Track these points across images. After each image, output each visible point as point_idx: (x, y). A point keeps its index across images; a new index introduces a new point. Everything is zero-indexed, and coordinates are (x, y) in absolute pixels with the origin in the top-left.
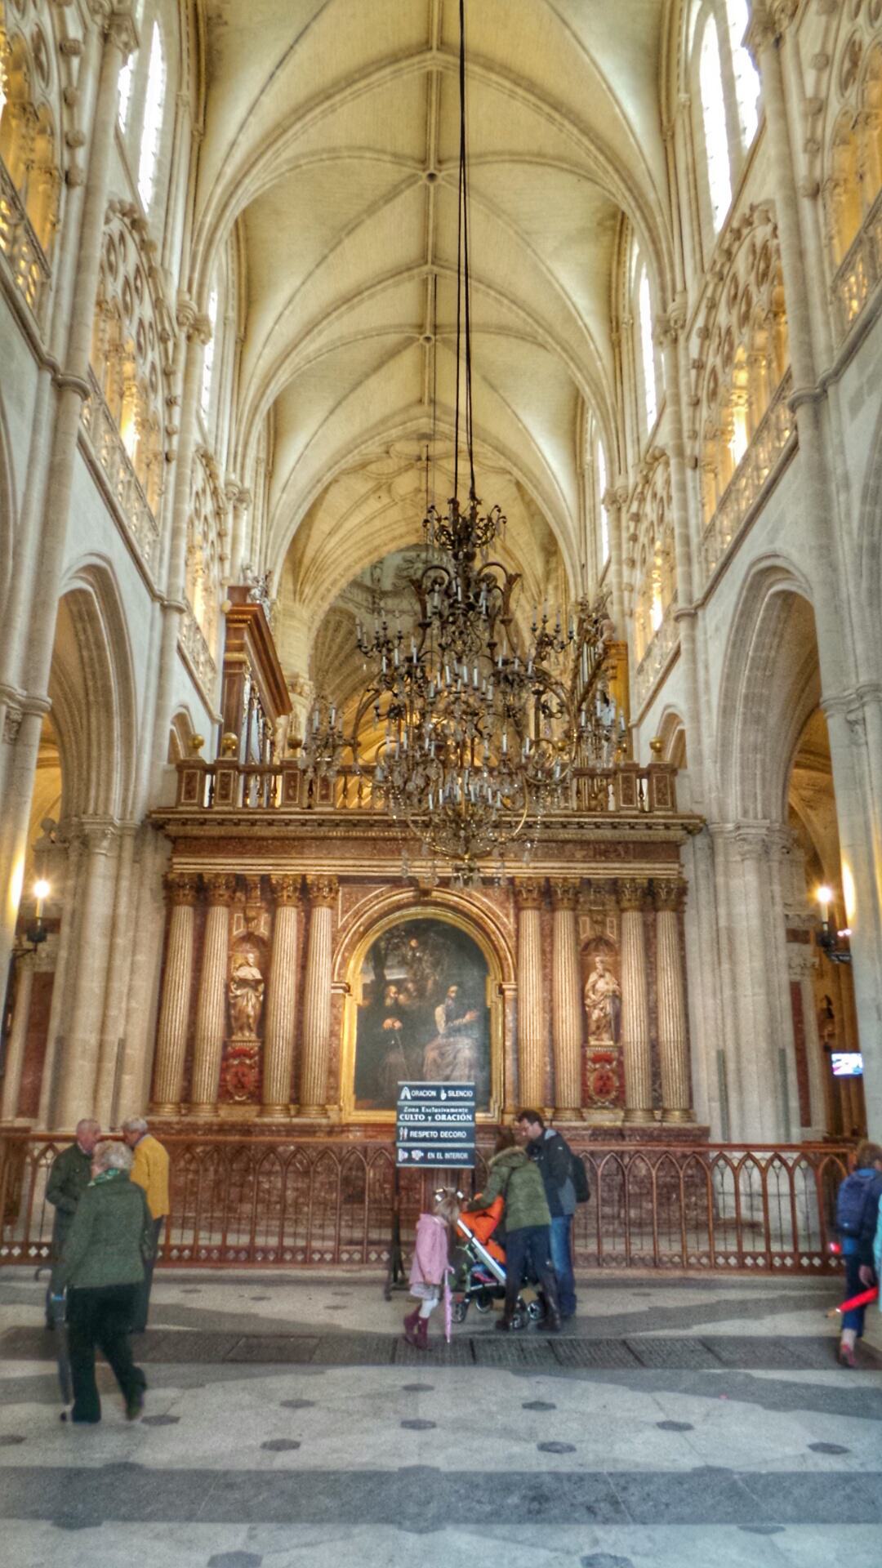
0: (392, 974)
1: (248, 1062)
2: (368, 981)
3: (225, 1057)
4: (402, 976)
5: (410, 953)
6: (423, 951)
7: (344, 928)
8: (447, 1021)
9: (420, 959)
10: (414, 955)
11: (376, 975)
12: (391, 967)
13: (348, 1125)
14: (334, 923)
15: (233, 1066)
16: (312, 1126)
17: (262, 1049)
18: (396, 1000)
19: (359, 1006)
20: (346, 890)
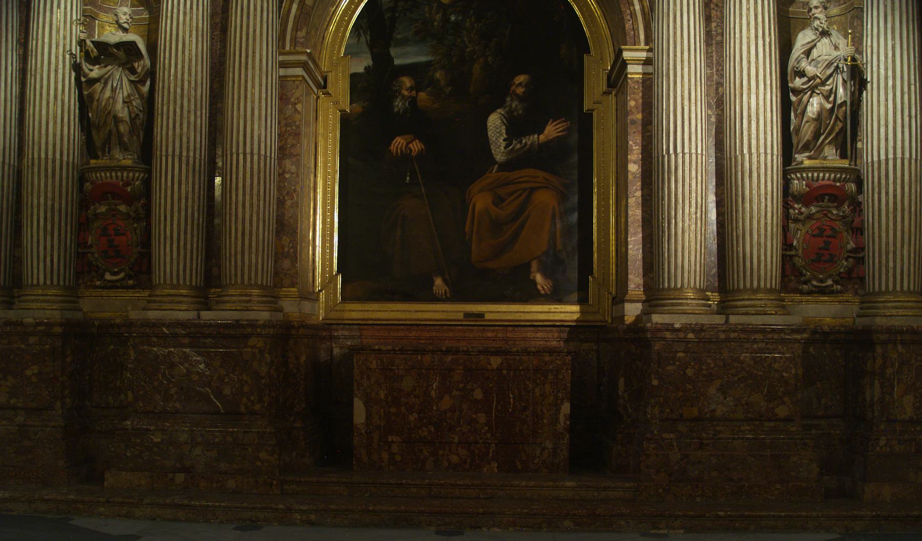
1: (123, 208)
2: (361, 70)
3: (84, 203)
4: (423, 59)
5: (438, 17)
8: (509, 141)
10: (446, 19)
12: (404, 42)
15: (97, 216)
16: (237, 324)
17: (147, 183)
18: (413, 101)
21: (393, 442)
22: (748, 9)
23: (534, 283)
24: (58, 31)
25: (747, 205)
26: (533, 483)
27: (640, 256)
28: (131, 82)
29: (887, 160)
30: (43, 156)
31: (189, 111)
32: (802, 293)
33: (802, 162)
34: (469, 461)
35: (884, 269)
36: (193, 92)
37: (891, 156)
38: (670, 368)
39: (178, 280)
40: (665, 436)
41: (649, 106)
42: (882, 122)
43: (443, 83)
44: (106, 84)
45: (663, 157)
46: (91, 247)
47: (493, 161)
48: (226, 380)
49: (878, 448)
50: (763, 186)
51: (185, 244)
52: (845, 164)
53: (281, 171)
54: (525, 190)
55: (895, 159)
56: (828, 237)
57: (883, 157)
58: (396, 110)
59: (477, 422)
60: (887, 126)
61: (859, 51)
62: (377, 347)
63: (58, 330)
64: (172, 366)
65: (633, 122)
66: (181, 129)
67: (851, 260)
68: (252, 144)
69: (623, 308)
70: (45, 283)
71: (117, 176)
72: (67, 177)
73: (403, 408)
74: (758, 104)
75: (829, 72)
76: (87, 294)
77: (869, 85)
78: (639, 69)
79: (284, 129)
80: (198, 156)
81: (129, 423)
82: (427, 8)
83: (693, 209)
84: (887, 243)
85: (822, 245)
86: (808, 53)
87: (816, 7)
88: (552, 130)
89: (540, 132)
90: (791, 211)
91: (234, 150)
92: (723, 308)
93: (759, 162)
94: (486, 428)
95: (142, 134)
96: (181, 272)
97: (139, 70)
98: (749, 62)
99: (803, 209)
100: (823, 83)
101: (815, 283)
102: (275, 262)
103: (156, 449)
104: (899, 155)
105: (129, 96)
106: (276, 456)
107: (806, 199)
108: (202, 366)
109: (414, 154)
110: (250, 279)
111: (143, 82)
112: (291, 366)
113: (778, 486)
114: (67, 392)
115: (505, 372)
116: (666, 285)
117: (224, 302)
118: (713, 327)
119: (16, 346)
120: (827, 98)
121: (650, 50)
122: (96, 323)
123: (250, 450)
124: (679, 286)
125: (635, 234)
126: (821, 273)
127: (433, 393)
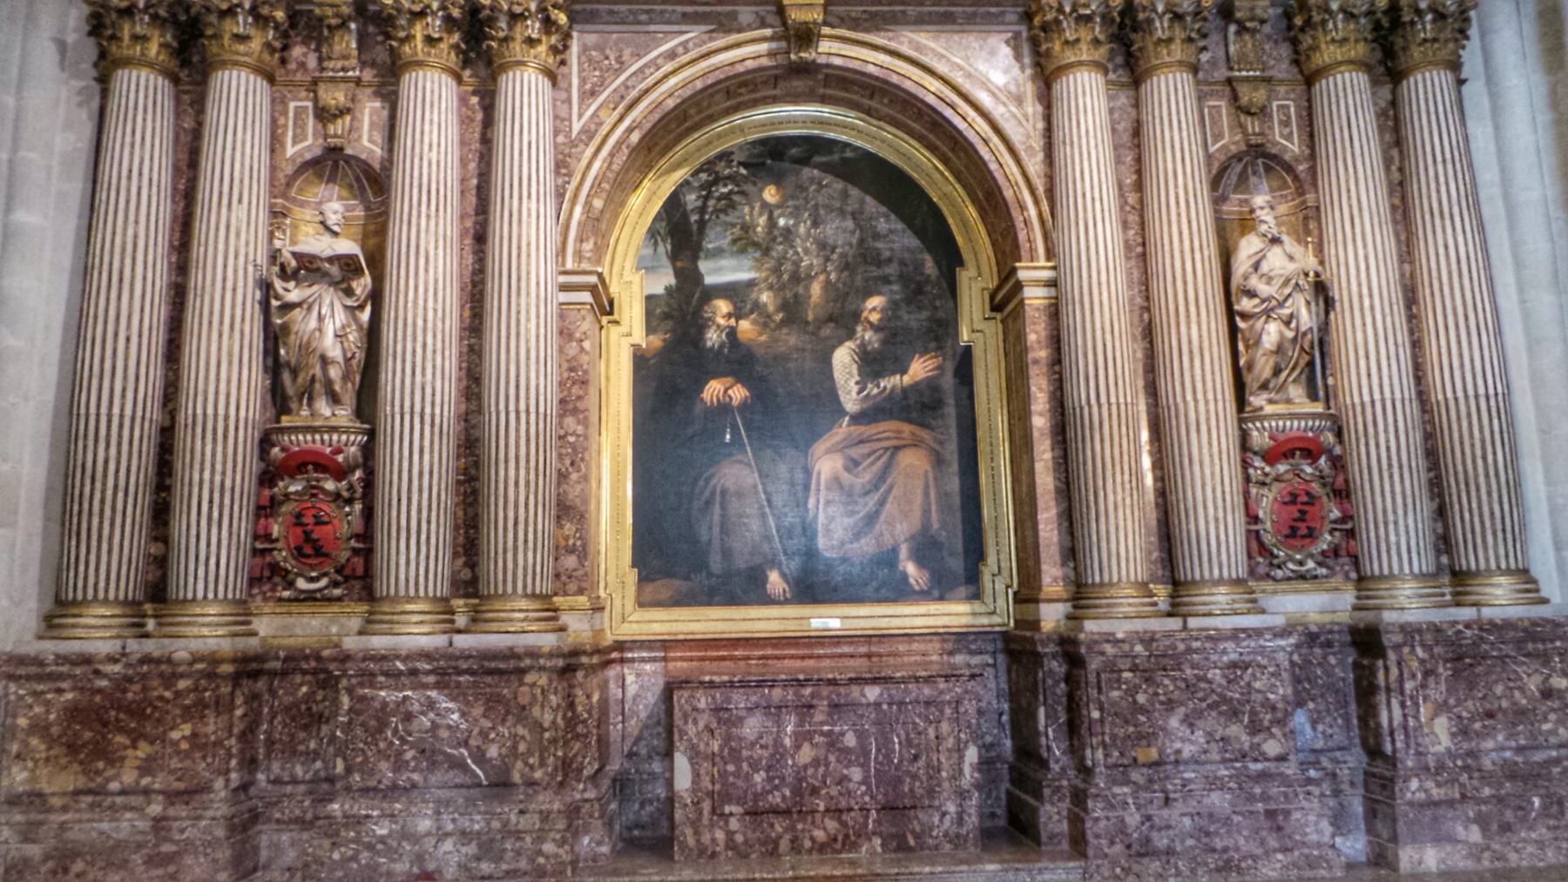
0: (718, 270)
1: (330, 485)
2: (659, 289)
3: (267, 477)
4: (744, 276)
5: (762, 220)
6: (796, 214)
7: (588, 134)
9: (788, 233)
10: (772, 223)
11: (678, 273)
12: (718, 253)
13: (620, 646)
14: (560, 122)
15: (287, 496)
16: (511, 654)
18: (732, 333)
19: (636, 347)
20: (591, 39)
21: (731, 814)
22: (1179, 215)
23: (905, 576)
24: (238, 235)
25: (1197, 468)
26: (940, 869)
27: (1055, 539)
28: (346, 307)
29: (1373, 402)
30: (210, 411)
31: (434, 352)
32: (1274, 579)
33: (1261, 408)
34: (840, 838)
36: (439, 324)
37: (1377, 396)
38: (1115, 694)
39: (417, 590)
40: (1117, 790)
41: (1056, 341)
42: (1361, 353)
43: (771, 308)
44: (309, 309)
45: (1081, 408)
46: (277, 540)
47: (841, 412)
48: (492, 736)
49: (1409, 795)
50: (1215, 443)
51: (428, 538)
52: (1319, 408)
53: (562, 432)
54: (887, 449)
55: (1383, 401)
56: (1303, 504)
57: (1367, 398)
58: (709, 344)
59: (850, 780)
60: (1367, 358)
61: (1322, 263)
62: (707, 678)
63: (226, 668)
64: (408, 717)
65: (1036, 362)
66: (424, 375)
67: (1337, 534)
68: (528, 398)
69: (1038, 610)
70: (205, 597)
71: (323, 441)
72: (245, 441)
73: (745, 766)
74: (1200, 336)
75: (1287, 291)
76: (267, 610)
77: (1338, 305)
78: (1041, 292)
79: (566, 375)
80: (446, 413)
81: (336, 806)
82: (747, 209)
83: (1127, 477)
84: (1385, 511)
85: (1297, 515)
86: (1256, 267)
88: (919, 369)
89: (904, 372)
90: (1251, 471)
92: (1173, 605)
93: (1208, 411)
94: (863, 788)
95: (358, 378)
96: (422, 579)
97: (358, 291)
98: (1185, 283)
99: (1267, 469)
100: (1281, 305)
101: (1291, 566)
102: (556, 559)
103: (380, 847)
104: (1388, 395)
105: (343, 327)
107: (1270, 457)
108: (455, 716)
109: (735, 403)
110: (525, 587)
111: (361, 307)
112: (580, 708)
113: (1280, 856)
114: (234, 762)
115: (885, 707)
116: (1097, 579)
117: (486, 621)
118: (1168, 635)
119: (155, 693)
120: (1287, 323)
121: (1054, 268)
122: (282, 654)
123: (528, 839)
124: (1115, 579)
125: (1047, 509)
126: (1299, 551)
127: (787, 742)
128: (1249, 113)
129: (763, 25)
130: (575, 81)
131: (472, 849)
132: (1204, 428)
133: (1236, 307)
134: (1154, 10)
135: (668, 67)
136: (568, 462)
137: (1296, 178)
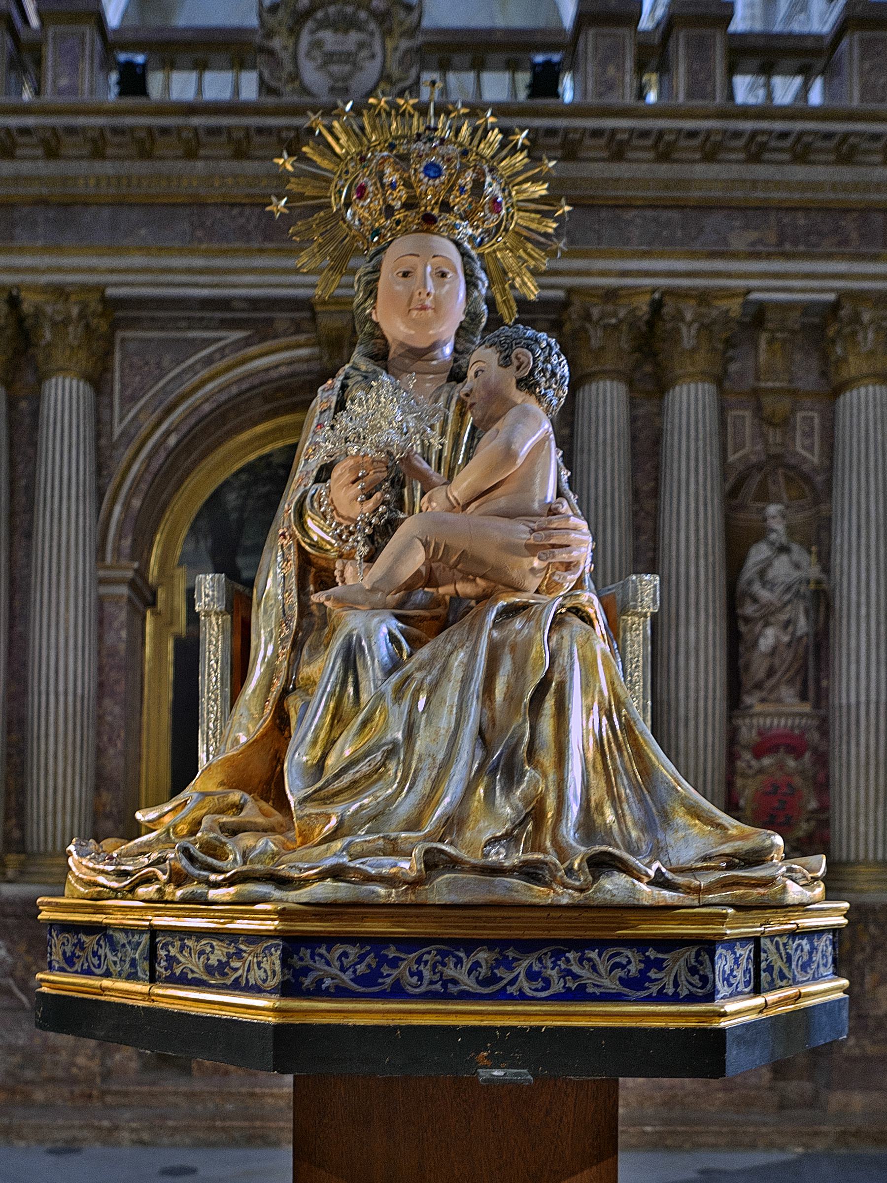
35: (853, 836)
37: (863, 698)
57: (853, 700)
61: (826, 569)
75: (787, 597)
84: (857, 804)
87: (774, 517)
91: (43, 688)
99: (754, 763)
100: (781, 609)
104: (873, 697)
106: (97, 1061)
113: (720, 1095)
123: (64, 1053)
128: (771, 424)
129: (298, 331)
130: (117, 387)
131: (16, 1059)
132: (692, 723)
133: (739, 611)
134: (683, 319)
135: (204, 373)
136: (105, 738)
137: (813, 489)
